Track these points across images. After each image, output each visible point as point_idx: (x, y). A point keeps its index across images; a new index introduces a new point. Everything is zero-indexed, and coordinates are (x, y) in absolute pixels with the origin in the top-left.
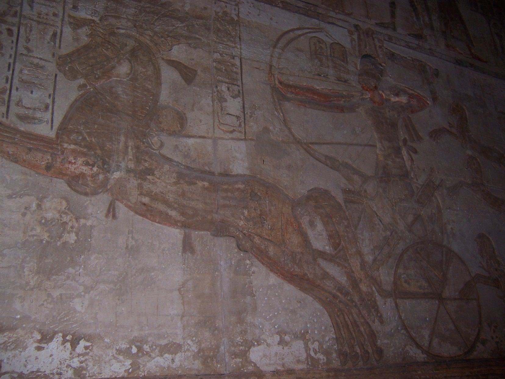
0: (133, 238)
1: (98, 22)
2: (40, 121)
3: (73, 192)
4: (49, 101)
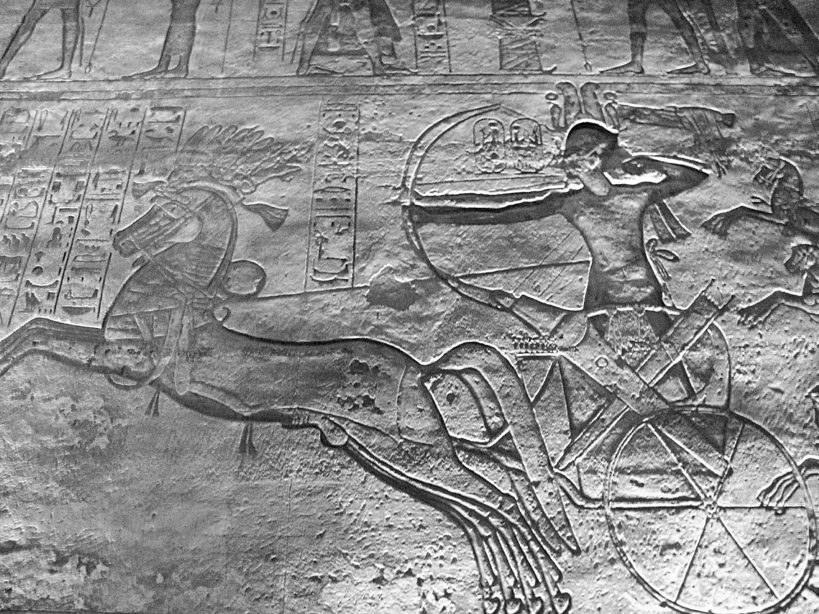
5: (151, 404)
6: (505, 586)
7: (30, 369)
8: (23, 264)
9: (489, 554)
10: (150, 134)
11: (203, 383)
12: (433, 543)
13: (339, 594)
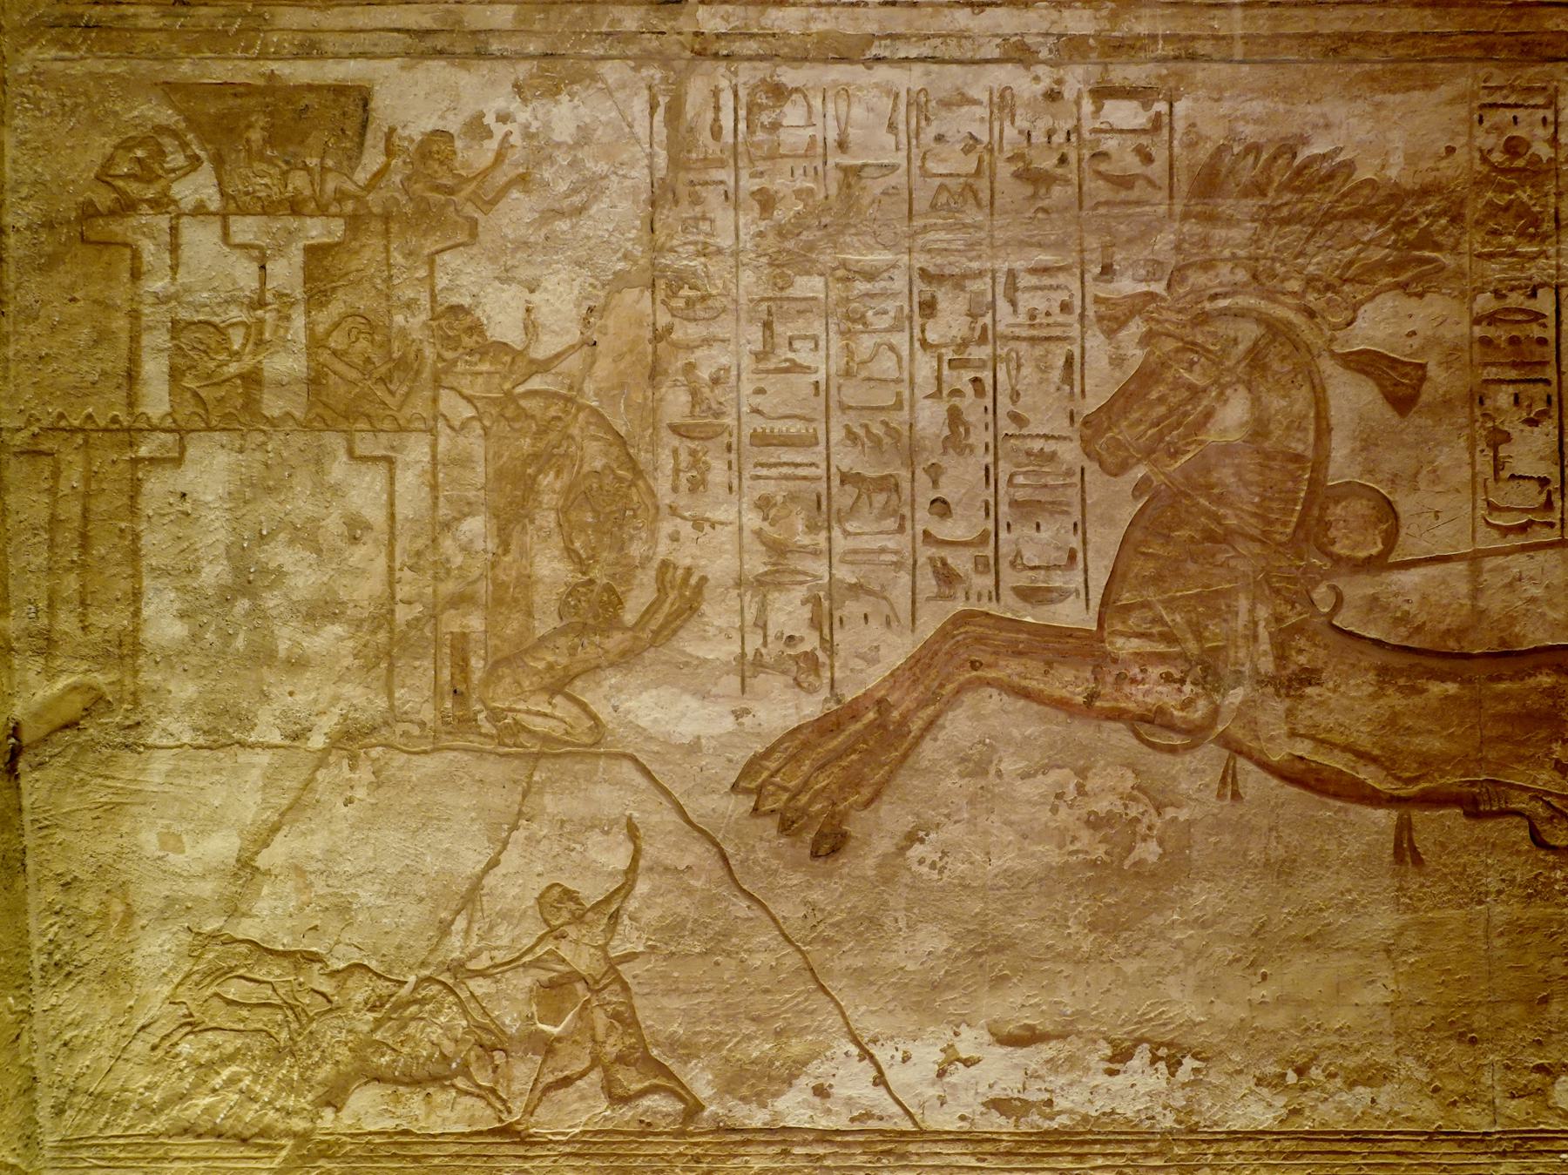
0: (1279, 837)
1: (1164, 293)
2: (1063, 594)
3: (1146, 749)
4: (1075, 542)
5: (1224, 778)
7: (978, 717)
10: (1103, 167)
11: (1313, 738)
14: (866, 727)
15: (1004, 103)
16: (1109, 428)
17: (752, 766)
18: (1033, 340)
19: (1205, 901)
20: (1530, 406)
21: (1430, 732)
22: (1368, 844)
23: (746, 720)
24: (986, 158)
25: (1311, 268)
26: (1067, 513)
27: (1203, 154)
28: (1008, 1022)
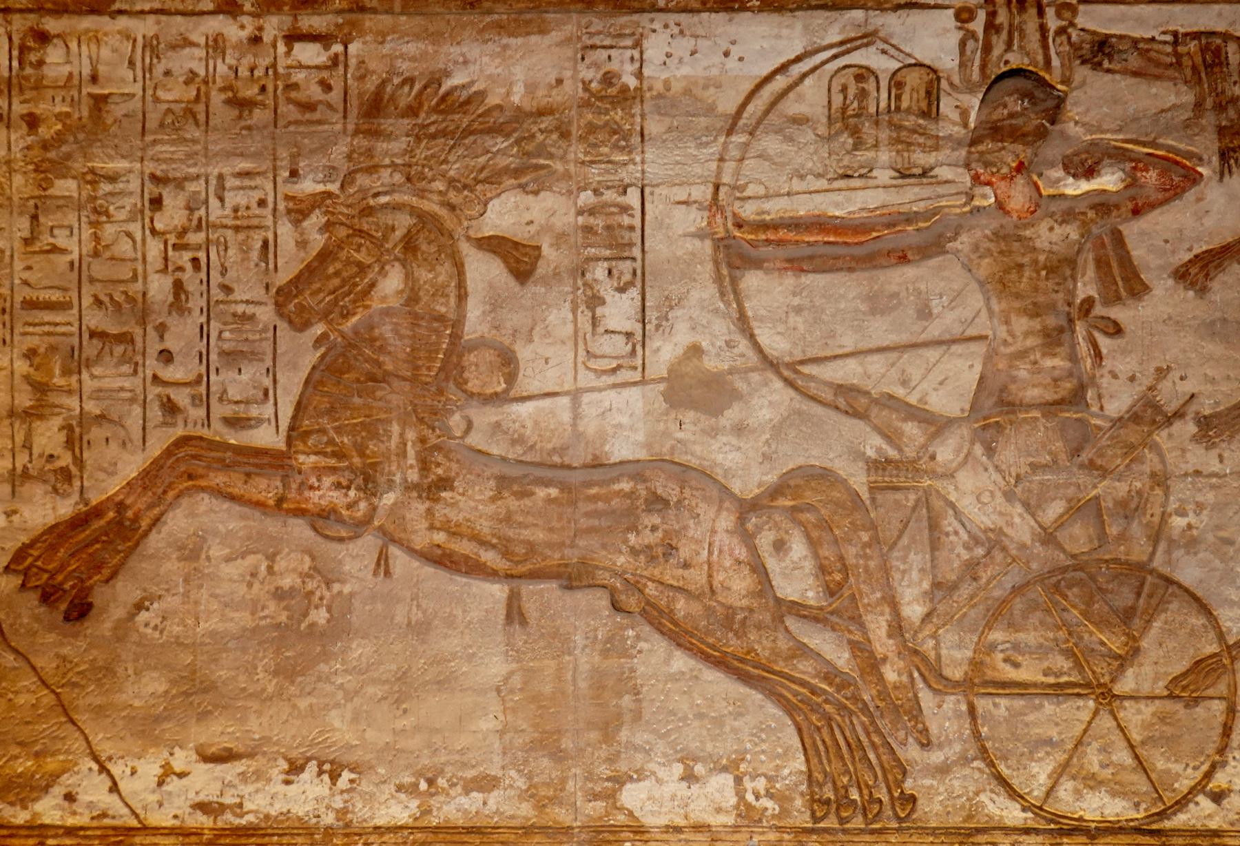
0: (418, 606)
1: (337, 192)
2: (260, 421)
3: (319, 539)
4: (267, 382)
5: (378, 564)
6: (839, 784)
7: (192, 514)
8: (139, 345)
9: (821, 748)
10: (293, 95)
12: (753, 735)
13: (642, 796)
14: (109, 523)
15: (217, 45)
16: (296, 296)
17: (20, 554)
18: (237, 229)
19: (361, 655)
20: (619, 278)
21: (536, 525)
22: (487, 611)
23: (15, 518)
24: (203, 89)
25: (452, 173)
26: (262, 360)
27: (371, 85)
28: (212, 745)
